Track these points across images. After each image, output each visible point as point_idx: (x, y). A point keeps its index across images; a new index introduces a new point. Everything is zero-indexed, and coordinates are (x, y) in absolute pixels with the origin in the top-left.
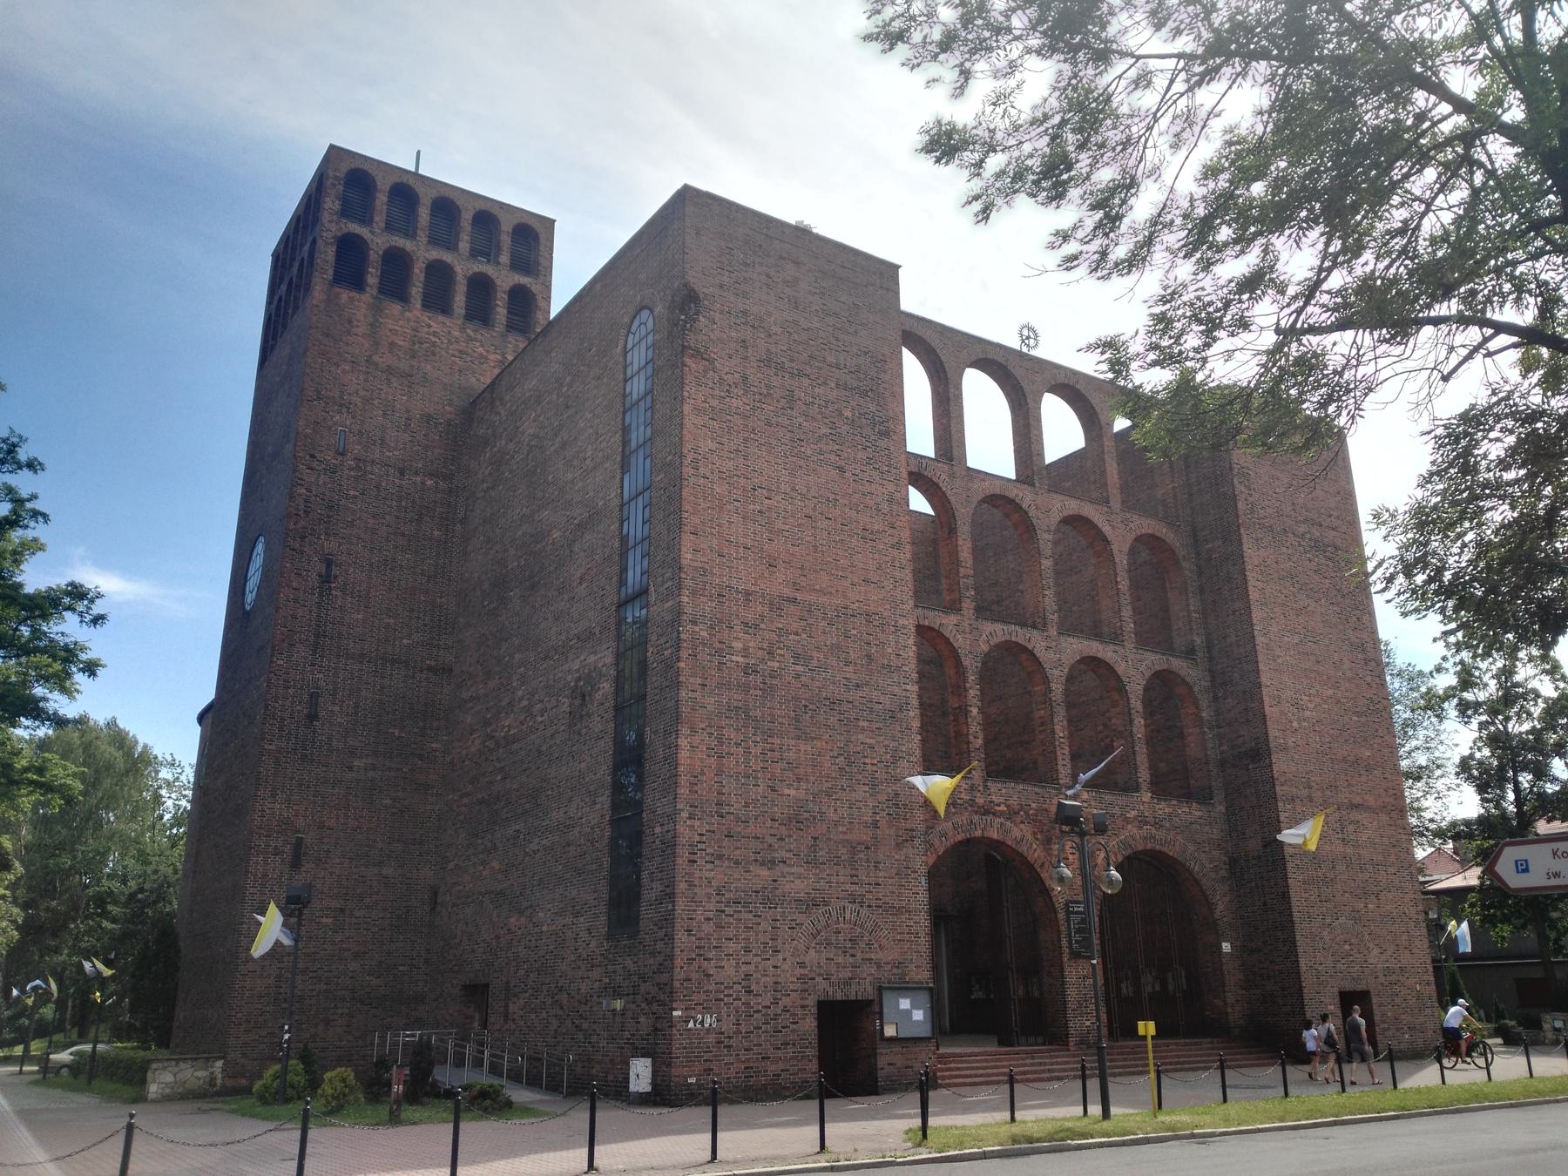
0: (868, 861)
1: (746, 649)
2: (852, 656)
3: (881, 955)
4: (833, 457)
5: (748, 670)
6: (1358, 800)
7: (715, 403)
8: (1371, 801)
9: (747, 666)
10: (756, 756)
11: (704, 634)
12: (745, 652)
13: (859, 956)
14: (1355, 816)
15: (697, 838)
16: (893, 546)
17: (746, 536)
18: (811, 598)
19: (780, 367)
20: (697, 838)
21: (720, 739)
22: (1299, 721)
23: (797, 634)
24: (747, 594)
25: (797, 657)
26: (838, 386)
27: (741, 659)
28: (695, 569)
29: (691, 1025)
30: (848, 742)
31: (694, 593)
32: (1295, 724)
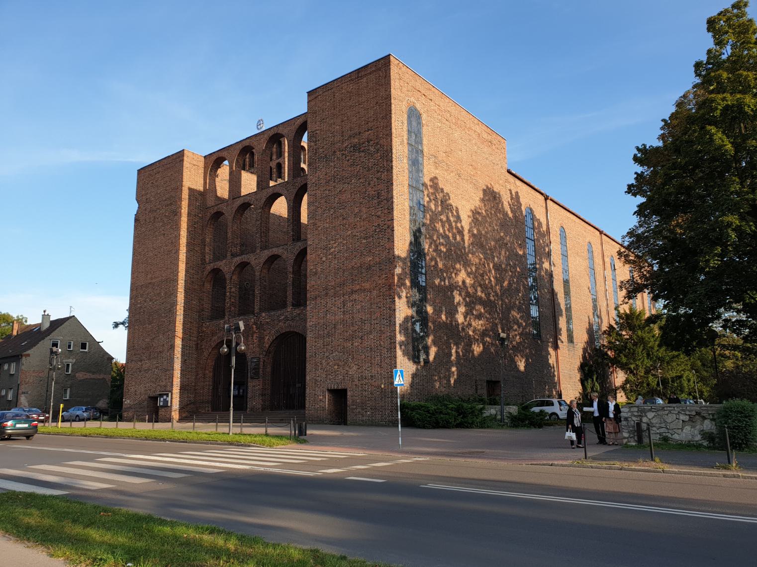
5: (141, 307)
6: (358, 287)
14: (355, 296)
32: (324, 259)
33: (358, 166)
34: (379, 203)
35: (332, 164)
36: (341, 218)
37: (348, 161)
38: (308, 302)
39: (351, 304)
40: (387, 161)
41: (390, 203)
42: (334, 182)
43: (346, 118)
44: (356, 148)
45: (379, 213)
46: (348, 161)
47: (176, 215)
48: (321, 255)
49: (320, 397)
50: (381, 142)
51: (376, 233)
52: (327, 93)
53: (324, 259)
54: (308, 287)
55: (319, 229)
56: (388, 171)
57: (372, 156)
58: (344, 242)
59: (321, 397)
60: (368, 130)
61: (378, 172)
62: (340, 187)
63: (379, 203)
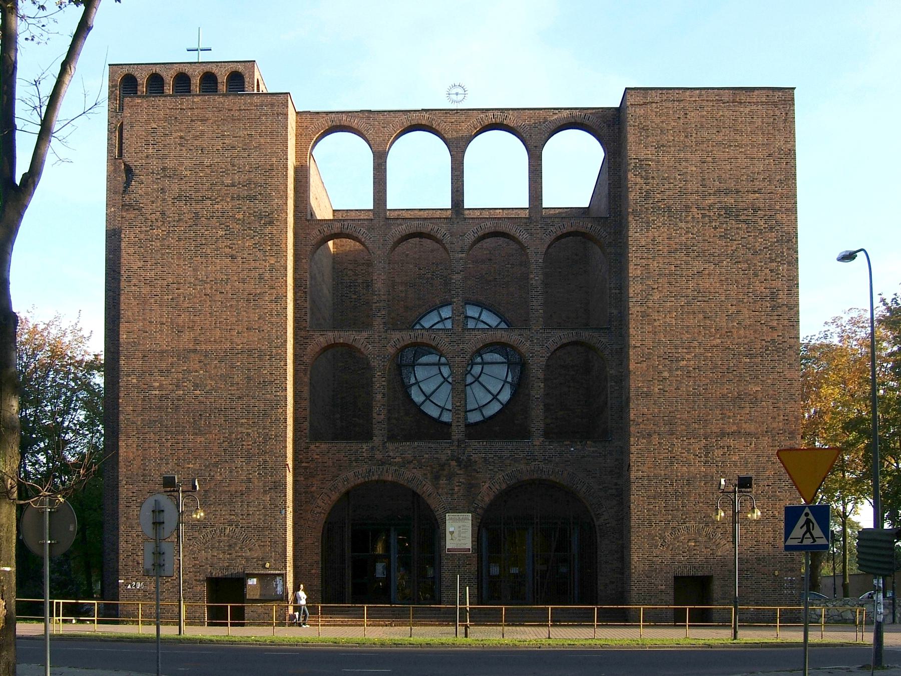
0: (242, 502)
1: (161, 386)
2: (236, 380)
3: (249, 554)
4: (228, 250)
5: (161, 398)
7: (142, 236)
8: (751, 427)
9: (162, 396)
10: (167, 448)
11: (135, 381)
12: (161, 387)
13: (234, 555)
15: (131, 495)
16: (271, 301)
17: (161, 316)
18: (203, 347)
19: (188, 199)
20: (131, 495)
21: (144, 440)
22: (670, 371)
23: (196, 371)
24: (162, 352)
25: (196, 386)
26: (233, 198)
27: (157, 392)
28: (128, 343)
29: (129, 587)
30: (231, 433)
31: (128, 358)
33: (736, 242)
34: (773, 308)
35: (683, 225)
36: (701, 316)
37: (715, 228)
38: (632, 439)
39: (721, 452)
40: (789, 249)
41: (792, 313)
42: (687, 255)
43: (710, 159)
44: (728, 212)
45: (775, 323)
46: (715, 228)
47: (271, 223)
48: (660, 367)
49: (660, 587)
50: (778, 217)
51: (768, 352)
52: (670, 105)
53: (666, 374)
54: (632, 415)
55: (656, 324)
56: (789, 263)
57: (761, 233)
58: (706, 354)
59: (663, 587)
60: (755, 192)
61: (772, 261)
62: (698, 265)
63: (773, 308)
